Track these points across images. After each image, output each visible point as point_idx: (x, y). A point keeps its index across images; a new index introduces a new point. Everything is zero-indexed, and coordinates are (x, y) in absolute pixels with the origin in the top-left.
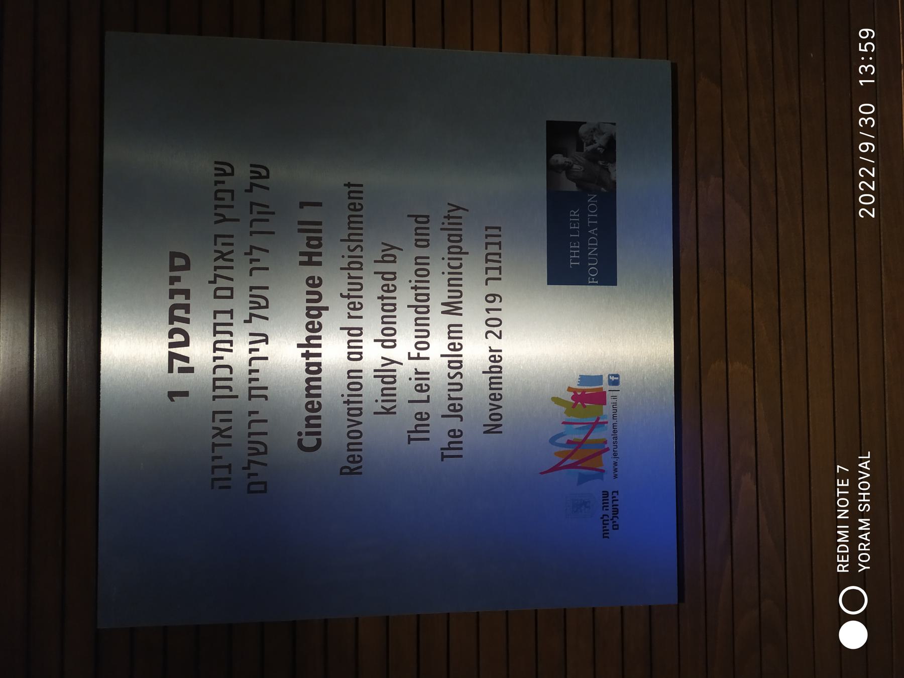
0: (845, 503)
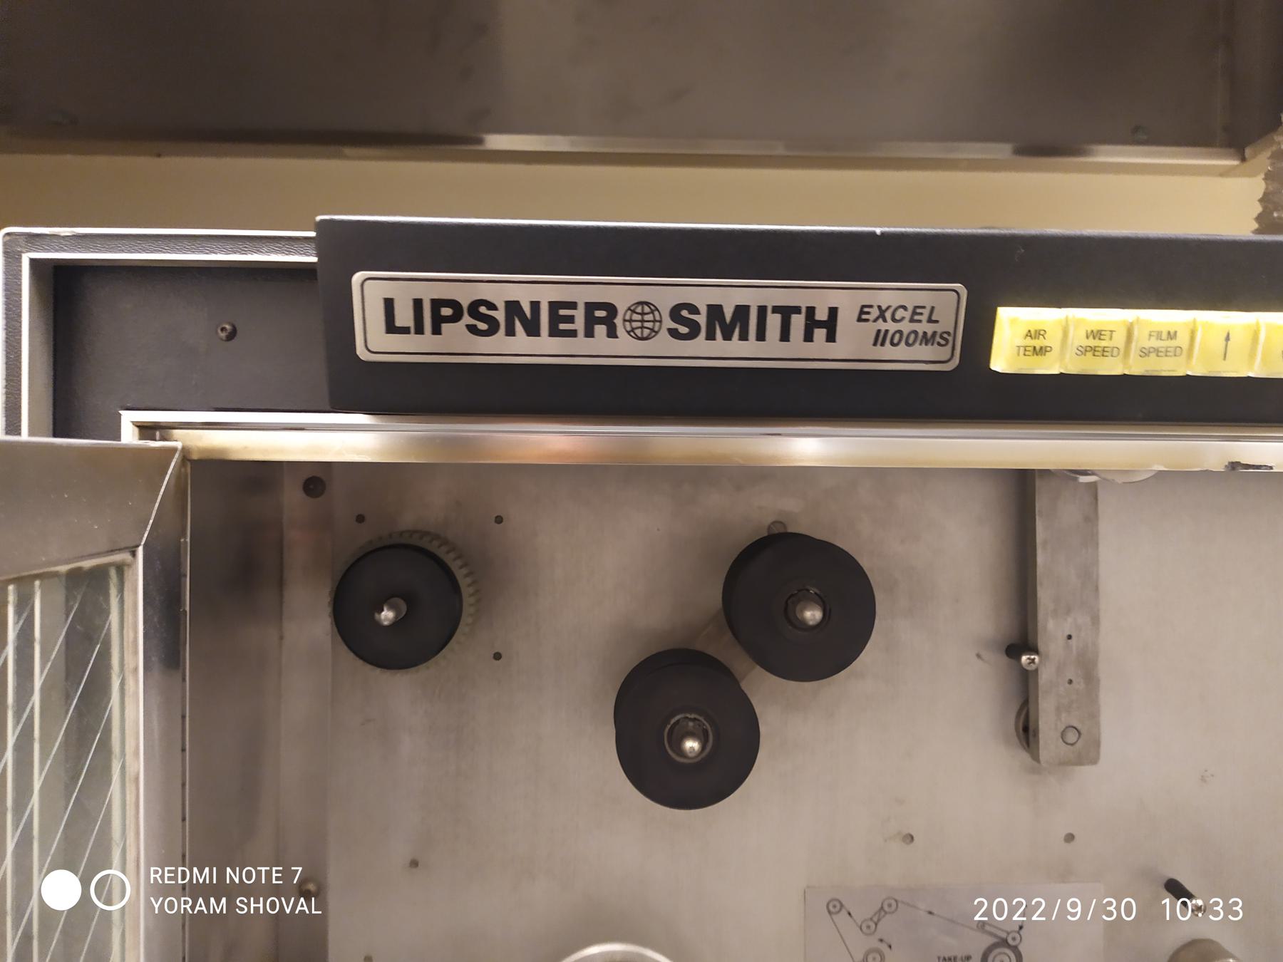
0: (249, 878)
